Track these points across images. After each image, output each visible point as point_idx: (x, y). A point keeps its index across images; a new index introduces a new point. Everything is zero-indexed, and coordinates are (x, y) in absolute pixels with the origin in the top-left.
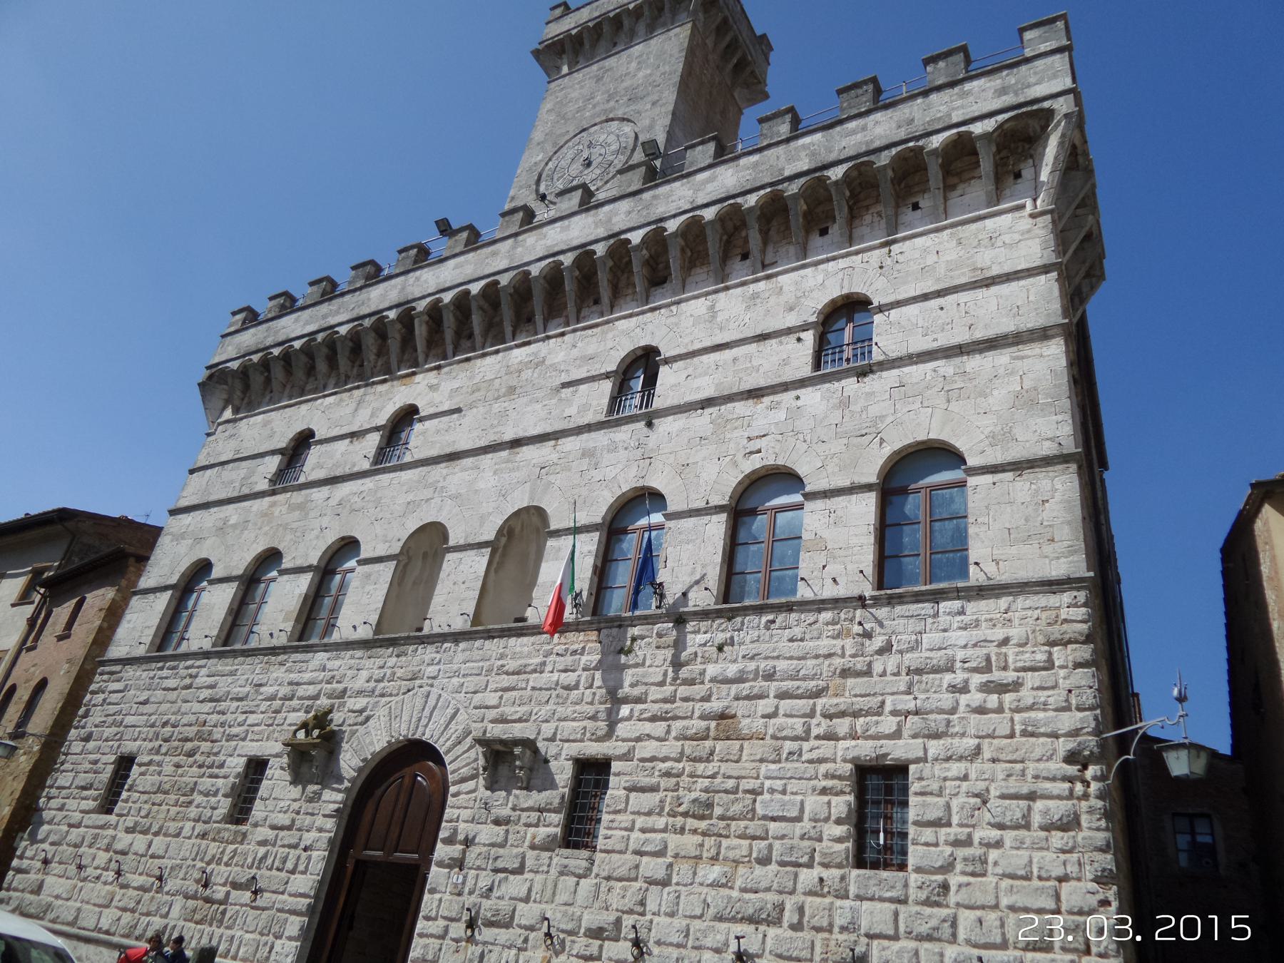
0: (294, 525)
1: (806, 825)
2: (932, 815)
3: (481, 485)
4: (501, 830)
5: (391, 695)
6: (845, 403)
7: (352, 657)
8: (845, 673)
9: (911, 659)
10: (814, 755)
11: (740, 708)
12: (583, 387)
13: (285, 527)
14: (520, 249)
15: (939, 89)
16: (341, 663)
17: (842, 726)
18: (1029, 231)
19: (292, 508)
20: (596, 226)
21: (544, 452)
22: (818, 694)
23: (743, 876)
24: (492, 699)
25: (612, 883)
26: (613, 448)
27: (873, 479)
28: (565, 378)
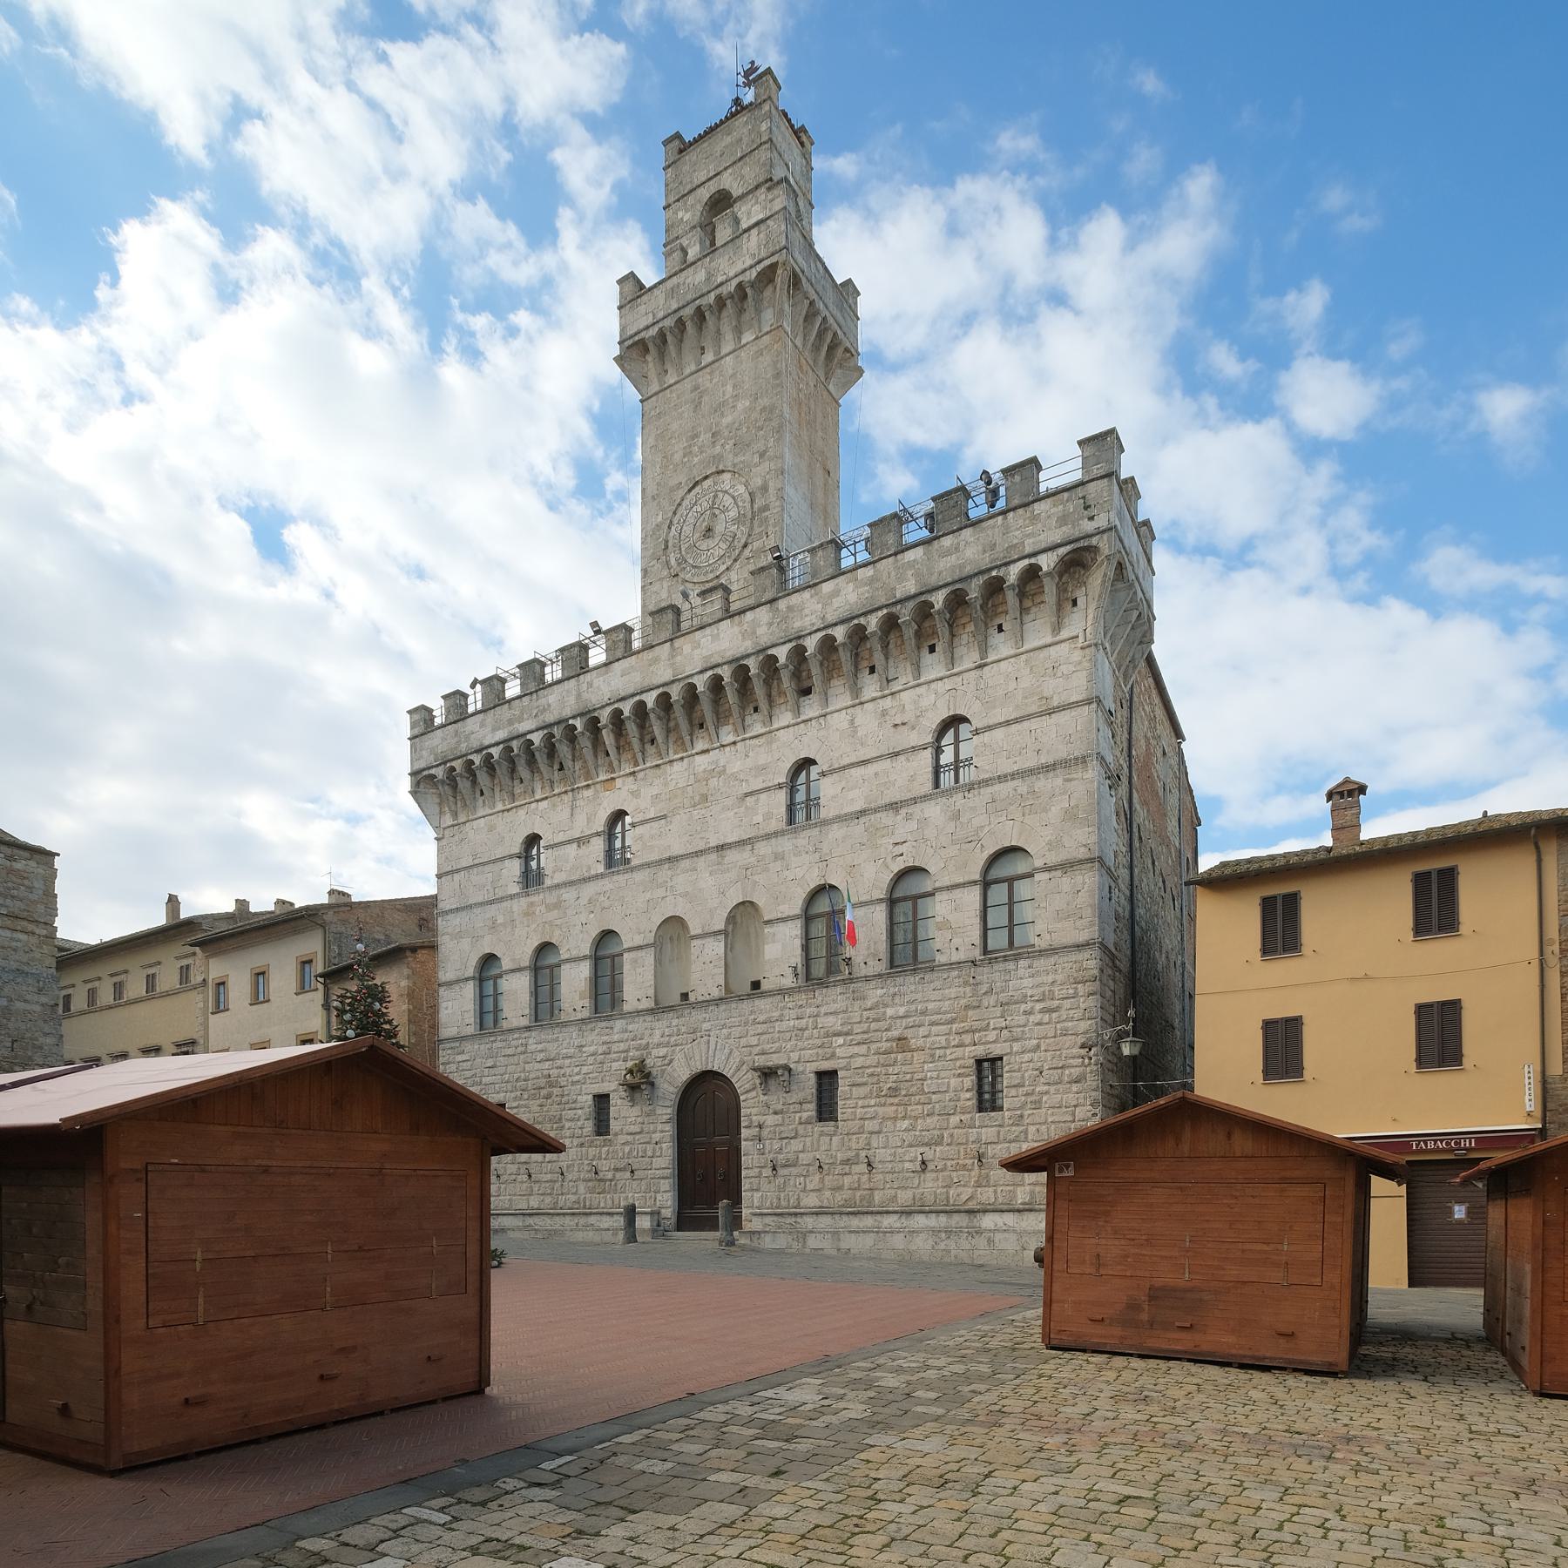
0: (558, 922)
4: (779, 1117)
8: (967, 1007)
11: (909, 1033)
12: (763, 796)
13: (551, 923)
17: (967, 1038)
19: (549, 908)
22: (952, 1021)
28: (745, 789)
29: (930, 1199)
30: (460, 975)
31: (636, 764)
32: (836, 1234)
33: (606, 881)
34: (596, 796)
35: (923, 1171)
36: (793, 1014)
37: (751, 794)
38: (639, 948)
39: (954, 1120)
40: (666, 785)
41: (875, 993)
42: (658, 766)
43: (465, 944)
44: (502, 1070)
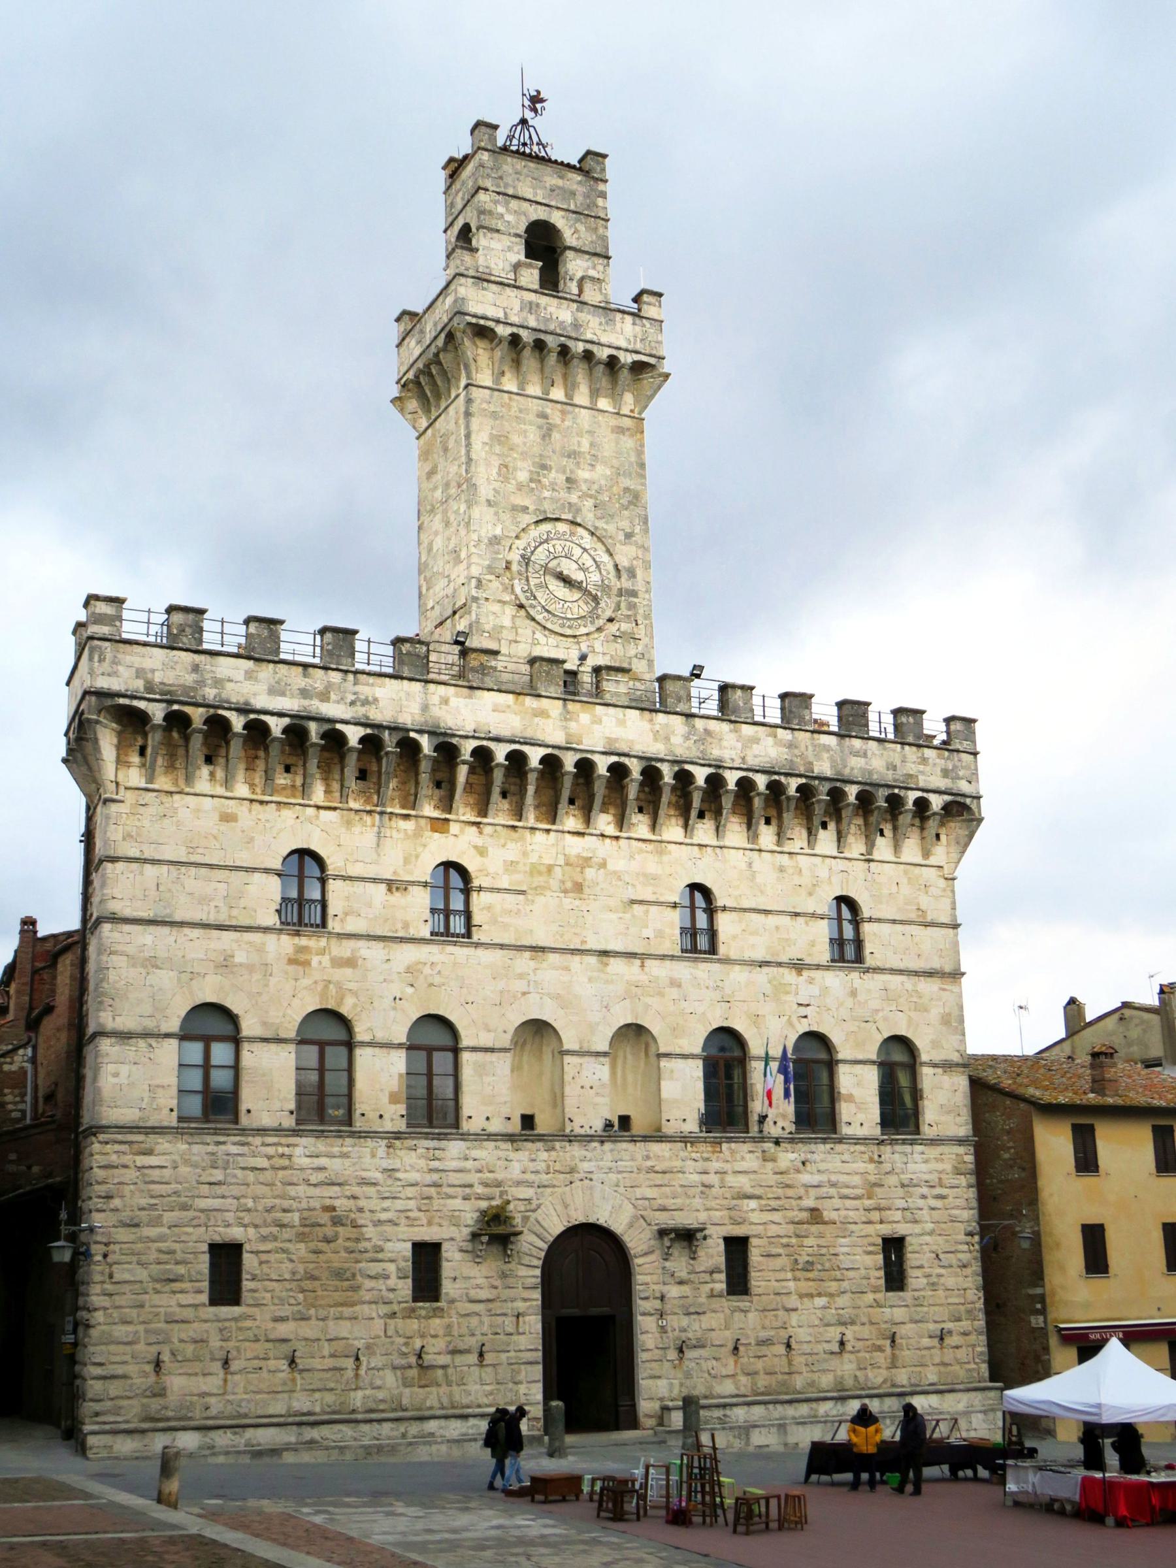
0: (351, 986)
1: (863, 1272)
2: (918, 1263)
5: (554, 1186)
6: (853, 993)
7: (496, 1148)
9: (905, 1178)
10: (863, 1234)
14: (573, 725)
15: (910, 744)
16: (486, 1153)
17: (875, 1216)
18: (944, 890)
19: (339, 963)
20: (656, 740)
23: (841, 1301)
24: (650, 1193)
25: (766, 1313)
27: (874, 1057)
29: (849, 1382)
30: (150, 1024)
31: (485, 816)
32: (782, 1428)
33: (434, 949)
34: (418, 834)
35: (840, 1353)
36: (700, 1165)
37: (641, 902)
38: (491, 1050)
40: (525, 854)
41: (787, 1157)
42: (514, 827)
43: (165, 978)
44: (236, 1190)
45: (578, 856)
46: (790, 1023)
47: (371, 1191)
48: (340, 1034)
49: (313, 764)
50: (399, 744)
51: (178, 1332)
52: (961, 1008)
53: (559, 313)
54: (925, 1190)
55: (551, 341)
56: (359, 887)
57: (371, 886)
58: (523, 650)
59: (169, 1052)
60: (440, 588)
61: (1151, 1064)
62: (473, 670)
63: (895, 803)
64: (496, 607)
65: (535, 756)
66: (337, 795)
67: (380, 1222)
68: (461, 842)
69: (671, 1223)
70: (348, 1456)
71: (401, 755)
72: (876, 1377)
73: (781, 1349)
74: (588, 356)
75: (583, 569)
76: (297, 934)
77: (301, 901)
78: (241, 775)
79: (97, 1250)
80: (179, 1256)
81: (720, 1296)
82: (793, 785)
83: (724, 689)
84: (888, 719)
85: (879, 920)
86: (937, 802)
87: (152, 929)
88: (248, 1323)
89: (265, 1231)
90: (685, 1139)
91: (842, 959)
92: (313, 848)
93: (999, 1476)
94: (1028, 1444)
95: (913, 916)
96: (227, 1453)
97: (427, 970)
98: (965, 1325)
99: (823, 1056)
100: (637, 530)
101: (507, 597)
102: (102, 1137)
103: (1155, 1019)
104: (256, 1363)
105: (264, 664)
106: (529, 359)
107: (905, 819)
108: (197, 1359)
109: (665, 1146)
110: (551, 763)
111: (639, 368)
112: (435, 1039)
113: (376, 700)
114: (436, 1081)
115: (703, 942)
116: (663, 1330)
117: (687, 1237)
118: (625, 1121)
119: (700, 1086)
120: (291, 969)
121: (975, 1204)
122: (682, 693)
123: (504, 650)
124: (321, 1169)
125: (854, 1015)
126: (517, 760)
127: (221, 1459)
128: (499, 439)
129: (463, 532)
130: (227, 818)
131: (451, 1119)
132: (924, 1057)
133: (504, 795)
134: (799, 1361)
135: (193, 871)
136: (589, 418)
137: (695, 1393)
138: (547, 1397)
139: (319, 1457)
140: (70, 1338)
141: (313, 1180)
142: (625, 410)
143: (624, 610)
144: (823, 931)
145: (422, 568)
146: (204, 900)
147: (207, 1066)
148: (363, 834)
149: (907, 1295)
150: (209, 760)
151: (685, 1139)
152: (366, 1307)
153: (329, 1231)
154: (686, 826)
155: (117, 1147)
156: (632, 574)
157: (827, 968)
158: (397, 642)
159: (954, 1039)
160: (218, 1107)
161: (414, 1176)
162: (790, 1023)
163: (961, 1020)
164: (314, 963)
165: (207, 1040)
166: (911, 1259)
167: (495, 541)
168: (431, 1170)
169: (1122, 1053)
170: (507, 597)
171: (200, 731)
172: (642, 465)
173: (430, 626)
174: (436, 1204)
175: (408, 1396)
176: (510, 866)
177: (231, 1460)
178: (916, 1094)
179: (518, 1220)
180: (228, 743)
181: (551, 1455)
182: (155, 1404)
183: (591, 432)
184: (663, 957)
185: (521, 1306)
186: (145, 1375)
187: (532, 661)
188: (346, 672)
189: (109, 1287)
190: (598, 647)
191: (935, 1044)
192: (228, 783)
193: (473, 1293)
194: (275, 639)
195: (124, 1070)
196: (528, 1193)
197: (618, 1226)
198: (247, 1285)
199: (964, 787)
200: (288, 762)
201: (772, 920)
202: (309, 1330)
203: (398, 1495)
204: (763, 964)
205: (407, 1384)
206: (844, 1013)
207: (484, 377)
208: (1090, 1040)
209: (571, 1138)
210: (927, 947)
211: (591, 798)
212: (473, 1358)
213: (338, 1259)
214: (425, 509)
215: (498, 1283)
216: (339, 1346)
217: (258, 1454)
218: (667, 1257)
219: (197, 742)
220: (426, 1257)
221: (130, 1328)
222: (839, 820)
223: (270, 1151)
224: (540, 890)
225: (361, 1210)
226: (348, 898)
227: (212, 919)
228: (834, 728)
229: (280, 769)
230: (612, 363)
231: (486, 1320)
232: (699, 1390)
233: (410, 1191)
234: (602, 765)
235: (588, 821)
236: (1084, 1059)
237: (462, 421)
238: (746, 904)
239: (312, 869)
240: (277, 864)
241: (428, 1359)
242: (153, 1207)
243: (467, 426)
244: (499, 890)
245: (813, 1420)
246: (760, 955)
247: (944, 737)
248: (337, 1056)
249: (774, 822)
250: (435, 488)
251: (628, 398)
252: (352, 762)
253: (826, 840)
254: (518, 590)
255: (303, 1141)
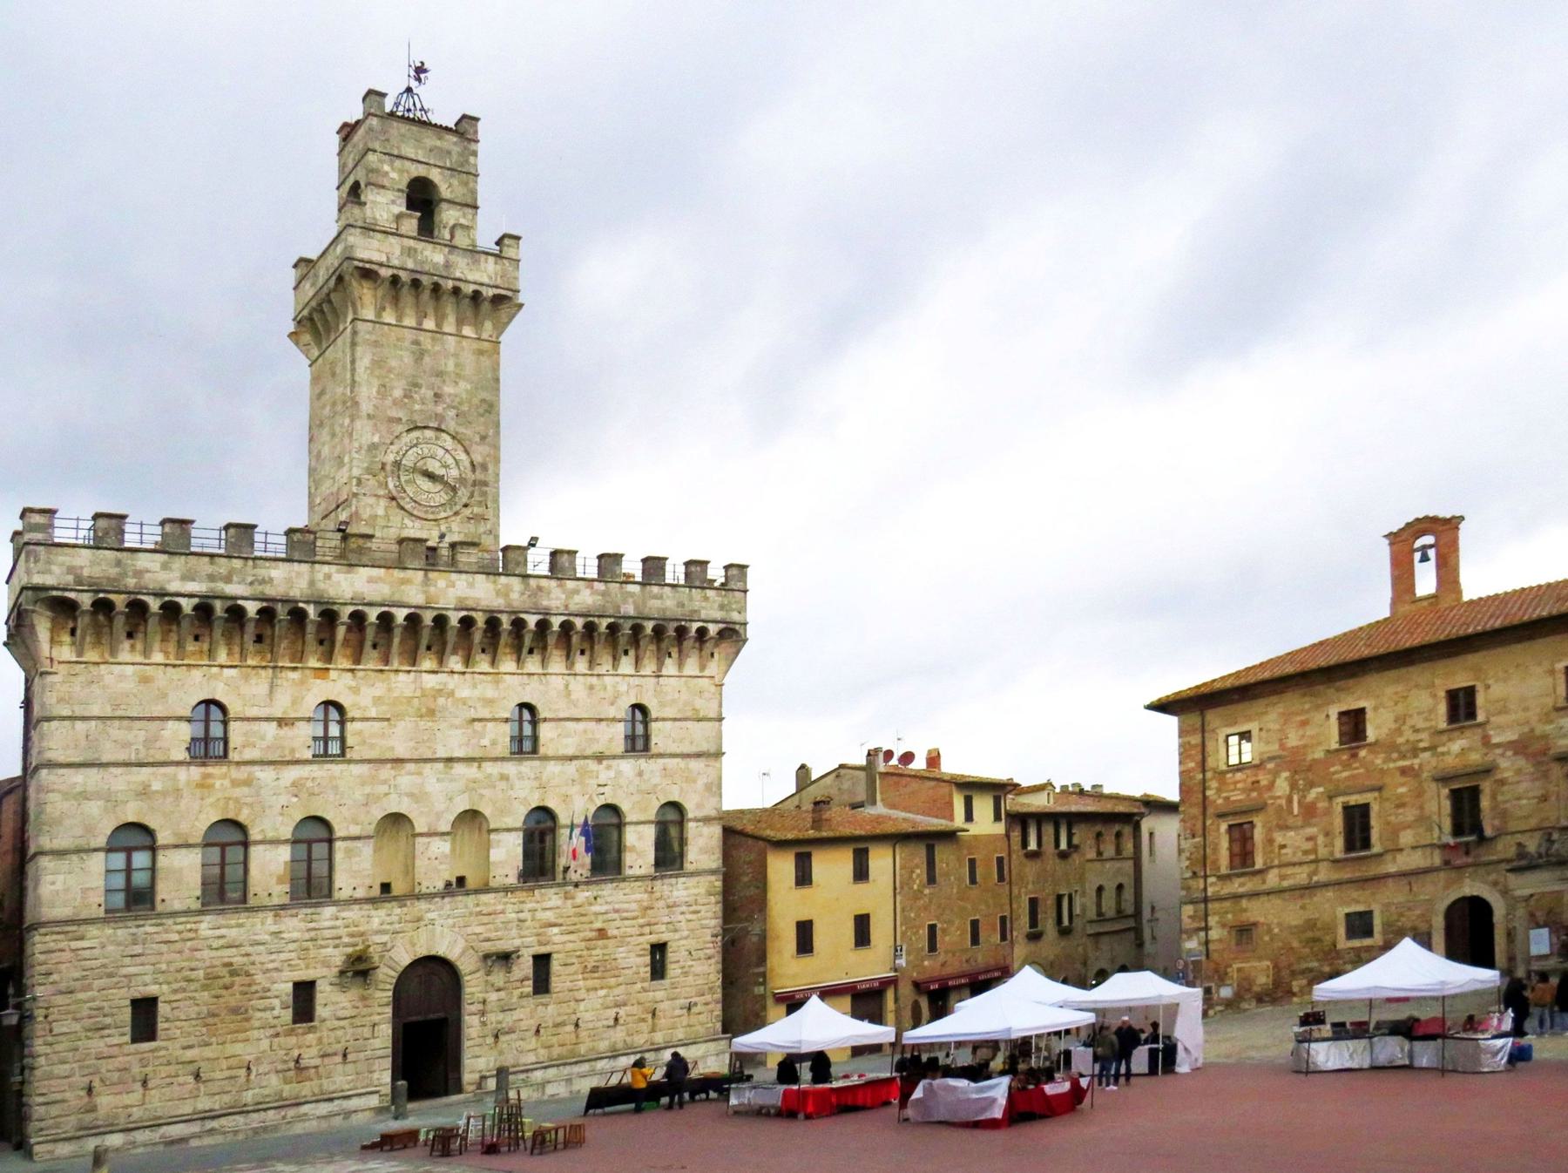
0: (249, 800)
3: (428, 788)
6: (640, 774)
9: (670, 901)
12: (490, 725)
13: (237, 800)
16: (354, 913)
17: (647, 930)
19: (235, 783)
21: (470, 771)
23: (617, 991)
24: (478, 930)
26: (521, 777)
29: (620, 1045)
30: (82, 842)
33: (315, 767)
34: (302, 682)
37: (480, 720)
39: (639, 986)
40: (389, 690)
41: (583, 895)
43: (94, 808)
44: (153, 959)
45: (432, 689)
46: (591, 798)
47: (261, 948)
48: (238, 837)
49: (218, 632)
50: (290, 613)
51: (104, 1066)
52: (720, 778)
53: (434, 256)
54: (684, 908)
55: (425, 280)
56: (256, 726)
57: (264, 725)
58: (393, 533)
59: (97, 862)
60: (326, 488)
61: (856, 806)
62: (352, 551)
63: (681, 632)
64: (372, 500)
65: (400, 615)
66: (237, 656)
67: (268, 971)
68: (339, 684)
69: (493, 949)
70: (241, 1137)
71: (291, 622)
72: (640, 1040)
73: (571, 1028)
74: (456, 291)
75: (446, 466)
76: (204, 764)
77: (207, 739)
78: (157, 646)
79: (39, 1014)
80: (107, 1010)
81: (528, 996)
82: (604, 623)
83: (555, 554)
84: (681, 570)
85: (664, 719)
86: (713, 629)
87: (82, 770)
88: (162, 1053)
89: (175, 986)
90: (507, 890)
91: (633, 750)
92: (217, 698)
93: (725, 1095)
94: (746, 1072)
95: (689, 714)
96: (145, 1145)
97: (309, 784)
98: (708, 998)
99: (615, 820)
100: (491, 432)
101: (382, 492)
102: (43, 931)
103: (862, 774)
104: (168, 1080)
105: (176, 558)
106: (407, 296)
107: (688, 644)
108: (121, 1082)
109: (492, 895)
110: (413, 620)
111: (498, 300)
112: (315, 833)
113: (271, 579)
114: (314, 865)
115: (527, 746)
116: (484, 1024)
117: (505, 958)
118: (461, 881)
119: (520, 850)
120: (198, 792)
121: (720, 914)
122: (521, 559)
123: (378, 534)
124: (223, 937)
125: (636, 789)
126: (386, 619)
127: (140, 1150)
128: (378, 363)
129: (346, 441)
130: (145, 680)
131: (325, 891)
132: (690, 815)
133: (375, 646)
134: (583, 1034)
135: (117, 723)
136: (454, 343)
137: (506, 1064)
138: (394, 1079)
139: (219, 1139)
140: (19, 1078)
141: (215, 945)
142: (485, 336)
143: (477, 498)
144: (620, 730)
145: (312, 471)
146: (126, 745)
147: (129, 870)
148: (258, 684)
149: (666, 982)
150: (130, 635)
151: (507, 890)
152: (255, 1032)
153: (227, 980)
154: (518, 660)
155: (55, 937)
156: (484, 467)
157: (622, 757)
158: (290, 532)
159: (713, 801)
160: (138, 899)
161: (295, 935)
162: (591, 798)
163: (720, 787)
164: (218, 784)
165: (129, 851)
166: (671, 956)
167: (373, 447)
168: (309, 930)
169: (836, 800)
170: (382, 492)
171: (122, 613)
172: (497, 380)
173: (317, 518)
174: (312, 953)
175: (288, 1090)
176: (377, 701)
177: (149, 1149)
178: (683, 842)
179: (376, 959)
180: (146, 621)
181: (396, 1118)
182: (88, 1118)
183: (456, 355)
184: (496, 759)
185: (376, 1018)
186: (81, 1098)
187: (401, 541)
188: (246, 559)
189: (50, 1039)
190: (455, 527)
191: (699, 806)
192: (146, 652)
193: (341, 1014)
194: (189, 537)
195: (61, 877)
196: (385, 938)
197: (452, 955)
198: (161, 1025)
199: (735, 616)
200: (197, 631)
201: (581, 726)
202: (208, 1052)
203: (279, 1159)
204: (571, 758)
205: (286, 1081)
206: (632, 789)
207: (368, 313)
208: (814, 792)
209: (419, 897)
210: (699, 736)
211: (444, 644)
212: (339, 1059)
213: (233, 999)
214: (316, 424)
215: (360, 1004)
216: (233, 1062)
217: (172, 1142)
218: (488, 973)
219: (120, 623)
220: (304, 994)
221: (67, 1066)
222: (637, 647)
223: (180, 927)
224: (400, 716)
225: (253, 963)
226: (245, 734)
227: (133, 758)
228: (639, 578)
229: (190, 639)
230: (476, 296)
231: (350, 1031)
232: (508, 1060)
233: (292, 946)
234: (454, 618)
235: (441, 662)
236: (808, 806)
237: (348, 350)
238: (562, 715)
239: (215, 713)
240: (187, 713)
241: (303, 1063)
242: (85, 978)
243: (353, 355)
244: (367, 719)
245: (592, 1073)
246: (570, 752)
247: (723, 580)
248: (235, 854)
249: (588, 653)
250: (324, 407)
251: (488, 325)
252: (250, 630)
253: (626, 665)
254: (391, 485)
255: (208, 918)
